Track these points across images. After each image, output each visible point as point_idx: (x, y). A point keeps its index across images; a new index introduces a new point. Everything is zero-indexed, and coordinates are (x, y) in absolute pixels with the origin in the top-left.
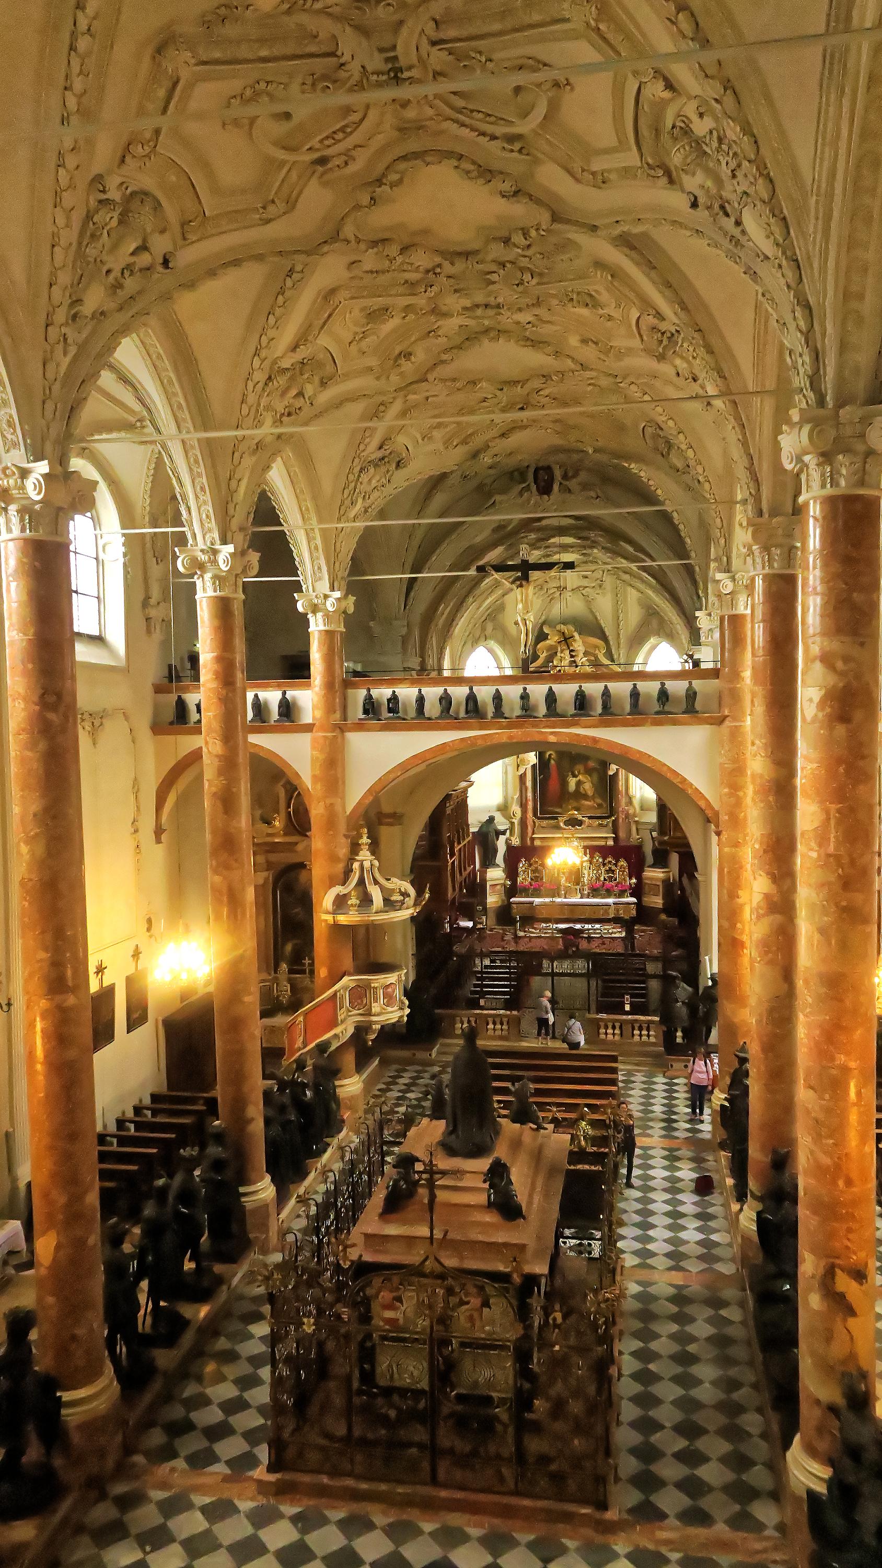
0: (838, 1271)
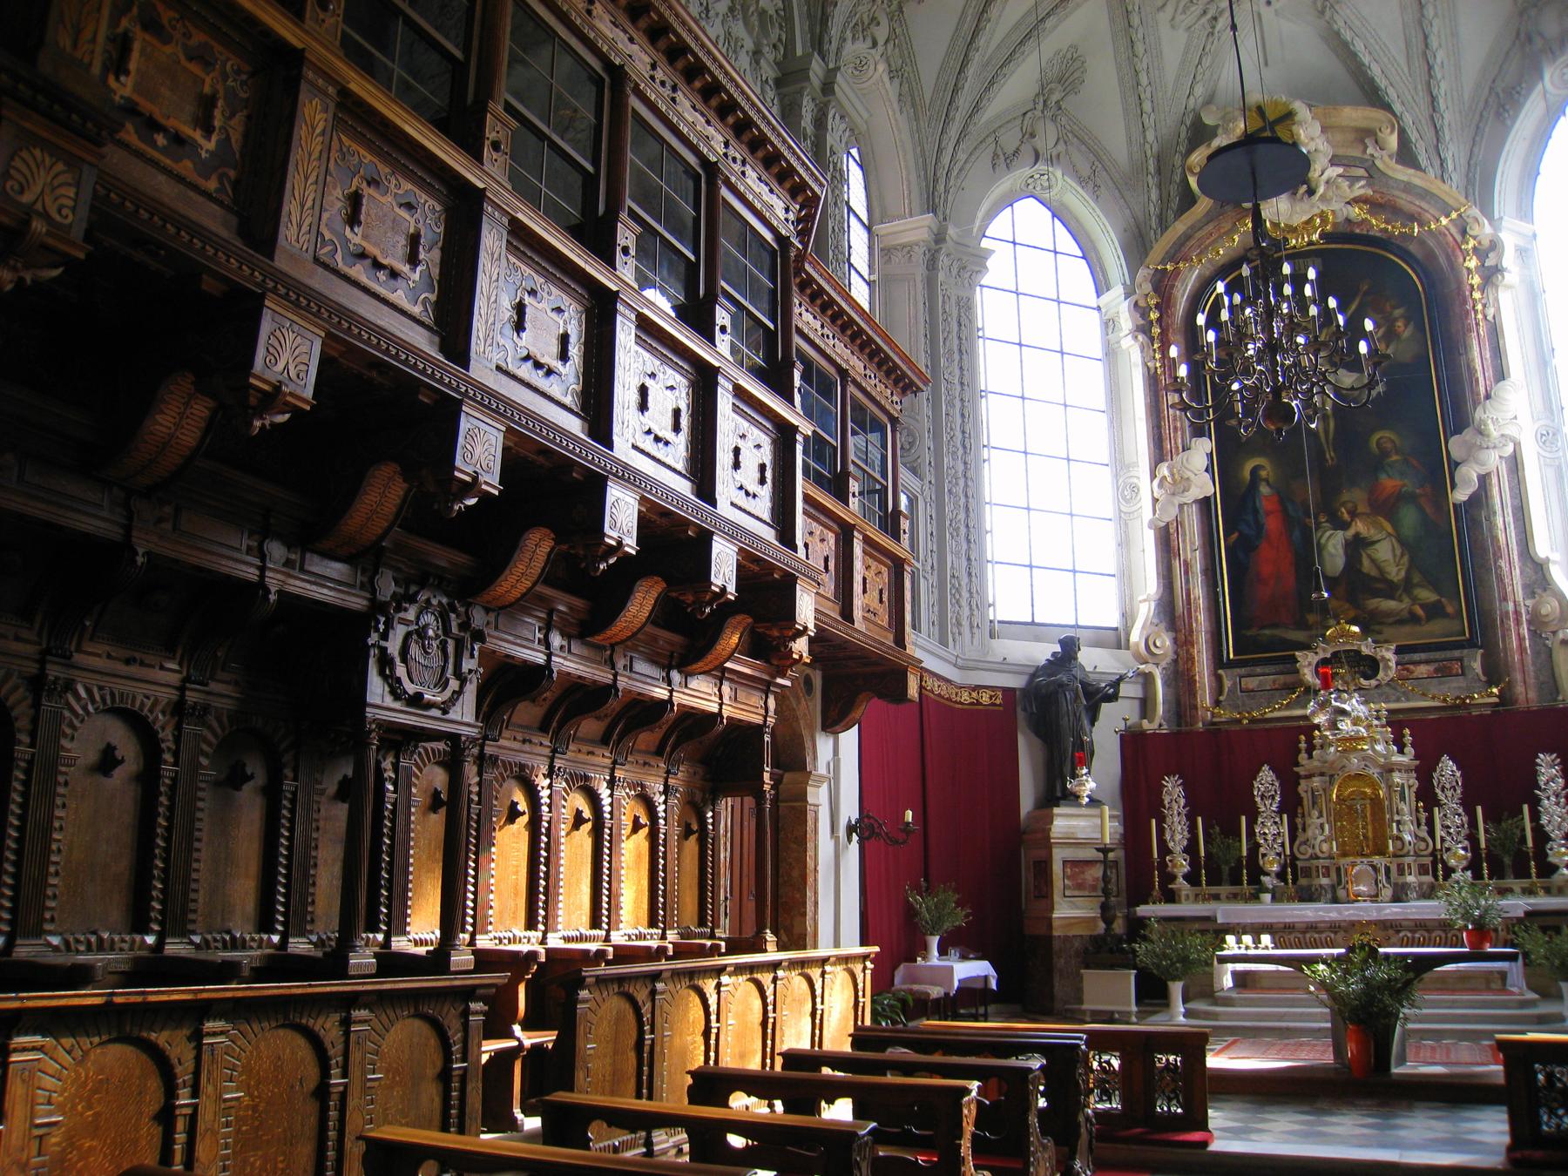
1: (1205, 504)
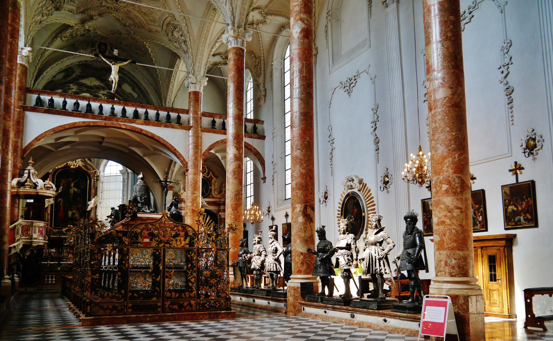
0: (308, 207)
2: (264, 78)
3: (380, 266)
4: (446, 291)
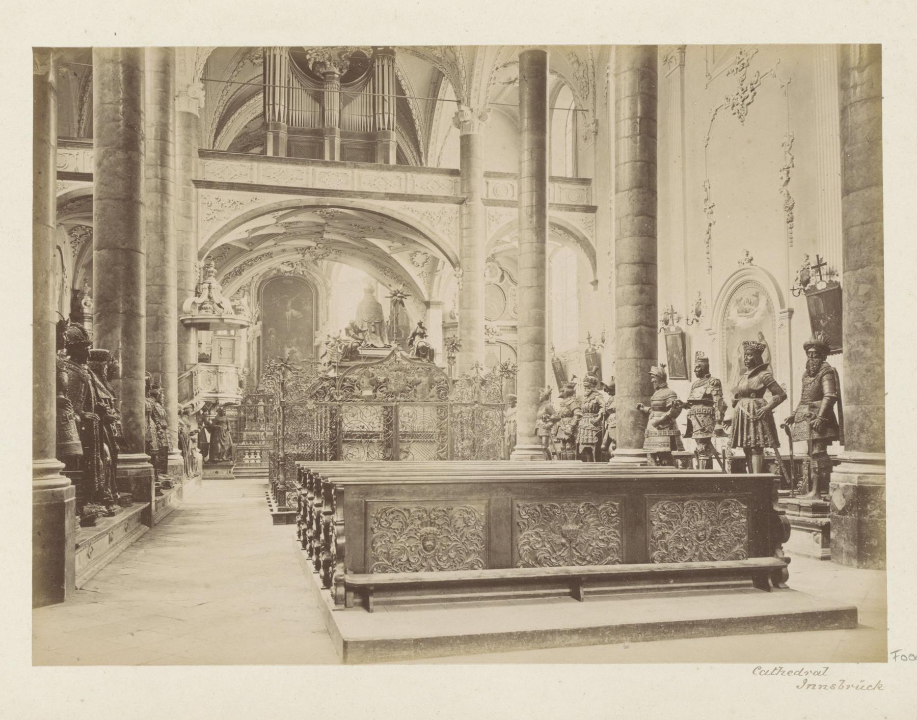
1: (258, 338)
2: (594, 99)
3: (756, 432)
4: (859, 478)
